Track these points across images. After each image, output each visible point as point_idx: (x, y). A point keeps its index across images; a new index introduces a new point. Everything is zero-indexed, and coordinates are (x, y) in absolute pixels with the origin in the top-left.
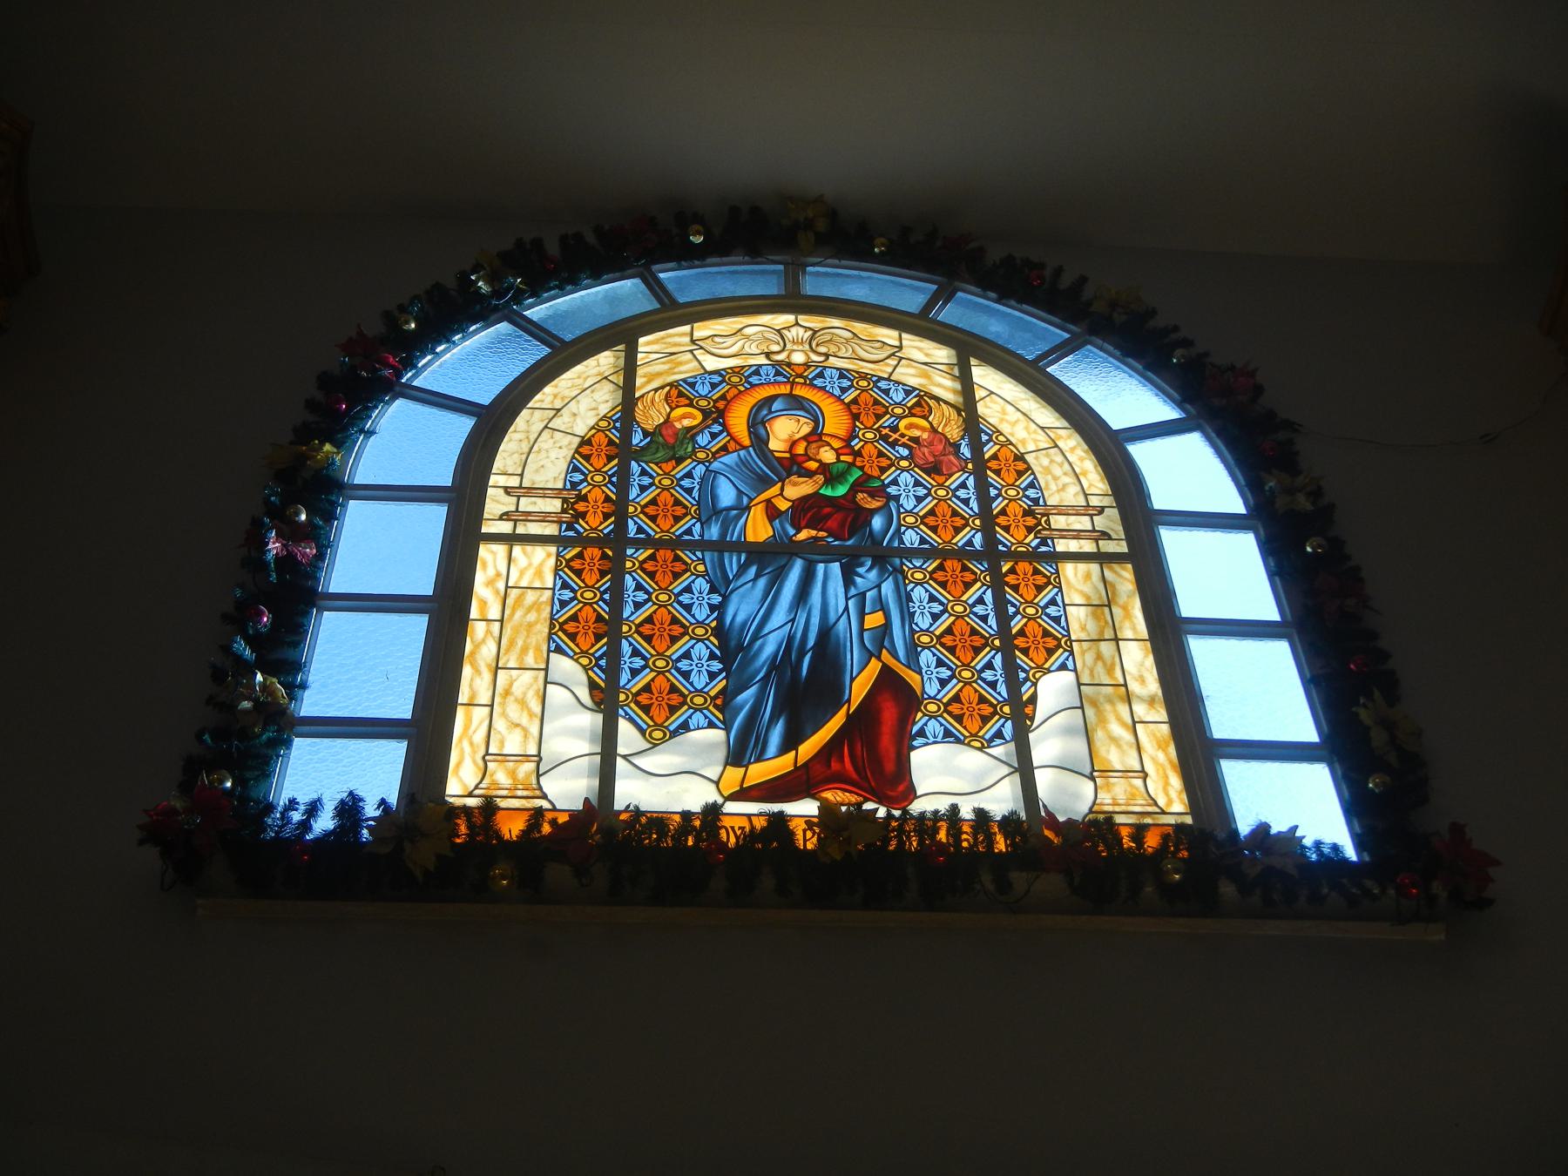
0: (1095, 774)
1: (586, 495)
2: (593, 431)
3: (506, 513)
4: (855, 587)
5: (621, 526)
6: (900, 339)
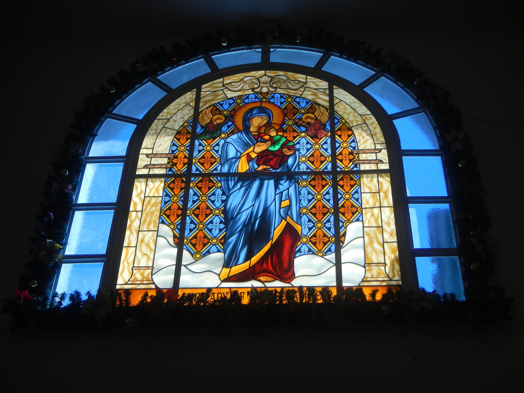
0: (366, 265)
1: (177, 156)
2: (182, 128)
3: (146, 165)
4: (279, 189)
5: (190, 168)
6: (306, 79)
